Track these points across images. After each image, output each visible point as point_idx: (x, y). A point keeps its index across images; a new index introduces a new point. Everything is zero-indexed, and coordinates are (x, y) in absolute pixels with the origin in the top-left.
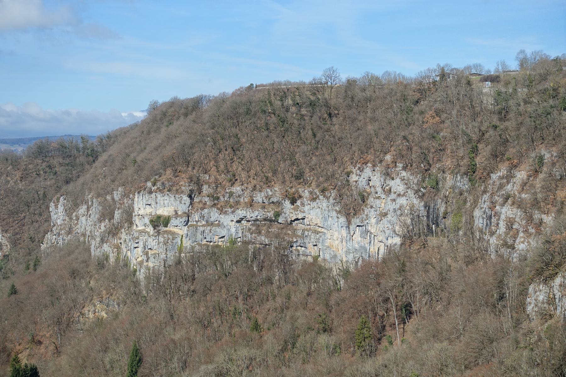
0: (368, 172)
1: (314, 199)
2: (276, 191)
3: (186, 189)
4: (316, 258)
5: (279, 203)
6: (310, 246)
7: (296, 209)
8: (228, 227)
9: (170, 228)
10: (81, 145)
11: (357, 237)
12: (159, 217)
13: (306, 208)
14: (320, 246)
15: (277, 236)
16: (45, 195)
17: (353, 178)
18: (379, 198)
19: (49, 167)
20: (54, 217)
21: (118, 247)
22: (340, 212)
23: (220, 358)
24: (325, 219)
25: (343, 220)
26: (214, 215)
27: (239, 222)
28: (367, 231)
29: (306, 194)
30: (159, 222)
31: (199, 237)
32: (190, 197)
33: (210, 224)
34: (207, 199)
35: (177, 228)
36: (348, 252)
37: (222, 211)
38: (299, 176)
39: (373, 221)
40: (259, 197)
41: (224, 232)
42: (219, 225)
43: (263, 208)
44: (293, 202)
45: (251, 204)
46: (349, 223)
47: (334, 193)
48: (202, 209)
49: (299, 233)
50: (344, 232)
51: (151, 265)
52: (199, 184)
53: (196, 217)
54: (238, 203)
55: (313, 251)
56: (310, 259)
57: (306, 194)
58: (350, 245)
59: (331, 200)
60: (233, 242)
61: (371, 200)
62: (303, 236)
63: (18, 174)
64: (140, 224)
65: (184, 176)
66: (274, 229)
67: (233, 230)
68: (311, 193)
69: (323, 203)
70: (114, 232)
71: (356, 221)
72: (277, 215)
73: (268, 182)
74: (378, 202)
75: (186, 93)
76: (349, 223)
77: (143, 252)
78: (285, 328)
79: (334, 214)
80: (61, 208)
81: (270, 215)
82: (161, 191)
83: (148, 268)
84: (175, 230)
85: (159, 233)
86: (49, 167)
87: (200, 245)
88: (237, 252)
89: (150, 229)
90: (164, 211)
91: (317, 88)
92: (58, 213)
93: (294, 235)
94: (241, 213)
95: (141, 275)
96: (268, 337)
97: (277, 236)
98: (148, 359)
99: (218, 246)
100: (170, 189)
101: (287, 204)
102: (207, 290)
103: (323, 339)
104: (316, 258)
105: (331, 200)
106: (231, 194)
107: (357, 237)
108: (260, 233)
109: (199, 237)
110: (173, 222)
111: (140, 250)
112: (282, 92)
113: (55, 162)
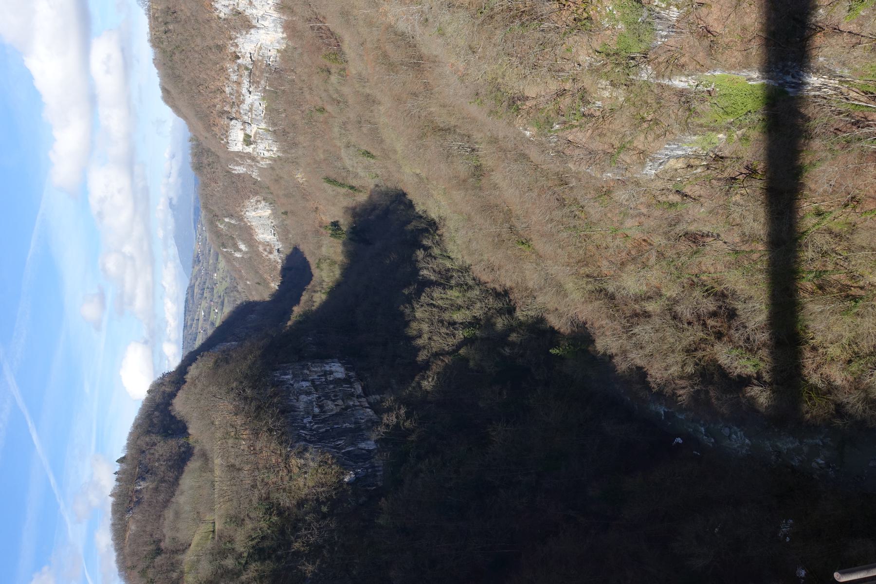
0: (217, 6)
1: (237, 46)
2: (231, 67)
3: (226, 121)
4: (278, 51)
5: (239, 66)
6: (270, 54)
7: (244, 57)
8: (253, 99)
9: (252, 134)
10: (194, 143)
11: (266, 23)
12: (244, 140)
13: (243, 50)
14: (270, 48)
15: (262, 72)
16: (228, 172)
17: (222, 15)
18: (238, 4)
19: (209, 165)
20: (241, 172)
21: (263, 158)
22: (247, 33)
23: (338, 143)
24: (252, 41)
25: (252, 31)
26: (245, 107)
27: (250, 93)
28: (262, 17)
29: (233, 49)
30: (248, 141)
31: (259, 118)
32: (231, 119)
33: (251, 110)
34: (234, 110)
35: (252, 130)
36: (276, 32)
37: (243, 102)
38: (221, 48)
39: (254, 11)
40: (234, 77)
41: (257, 103)
42: (252, 105)
43: (241, 76)
44: (239, 58)
45: (239, 84)
46: (254, 27)
47: (233, 33)
48: (240, 113)
49: (260, 58)
50: (261, 31)
51: (275, 149)
52: (222, 113)
53: (245, 118)
54: (237, 92)
55: (273, 53)
56: (279, 55)
57: (233, 49)
58: (271, 29)
59: (238, 35)
60: (263, 98)
61: (240, 9)
62: (263, 56)
63: (213, 184)
64: (249, 149)
65: (217, 121)
66: (257, 73)
67: (256, 97)
68: (232, 46)
69: (240, 41)
70: (253, 159)
71: (254, 22)
72: (247, 69)
73: (223, 69)
74: (240, 5)
75: (159, 93)
76: (254, 27)
77: (267, 150)
78: (324, 95)
79: (248, 36)
80: (236, 168)
81: (246, 73)
82: (227, 137)
83: (277, 151)
84: (254, 131)
85: (255, 142)
86: (209, 165)
87: (265, 118)
88: (271, 96)
89: (252, 146)
90: (241, 136)
91: (153, 19)
92: (239, 170)
93: (262, 61)
94: (244, 91)
95: (280, 155)
96: (329, 108)
97: (262, 72)
98: (333, 175)
99: (266, 108)
100: (226, 131)
101: (239, 61)
102: (294, 125)
103: (334, 79)
104: (278, 51)
105: (238, 35)
106: (231, 94)
107: (266, 23)
108: (258, 82)
109: (259, 118)
110: (248, 132)
111: (266, 153)
112: (156, 42)
113: (206, 162)
